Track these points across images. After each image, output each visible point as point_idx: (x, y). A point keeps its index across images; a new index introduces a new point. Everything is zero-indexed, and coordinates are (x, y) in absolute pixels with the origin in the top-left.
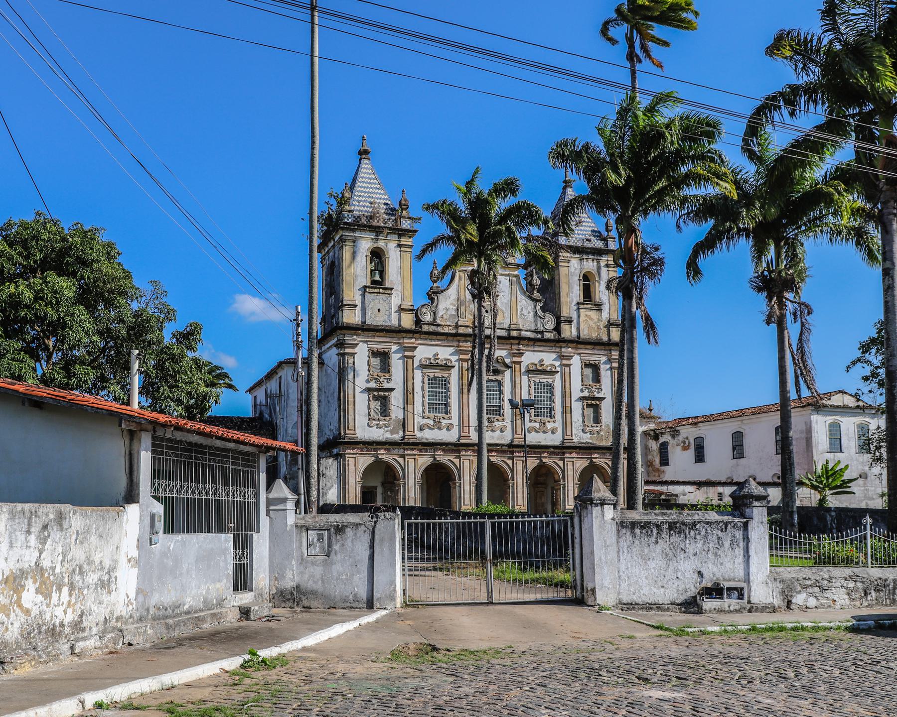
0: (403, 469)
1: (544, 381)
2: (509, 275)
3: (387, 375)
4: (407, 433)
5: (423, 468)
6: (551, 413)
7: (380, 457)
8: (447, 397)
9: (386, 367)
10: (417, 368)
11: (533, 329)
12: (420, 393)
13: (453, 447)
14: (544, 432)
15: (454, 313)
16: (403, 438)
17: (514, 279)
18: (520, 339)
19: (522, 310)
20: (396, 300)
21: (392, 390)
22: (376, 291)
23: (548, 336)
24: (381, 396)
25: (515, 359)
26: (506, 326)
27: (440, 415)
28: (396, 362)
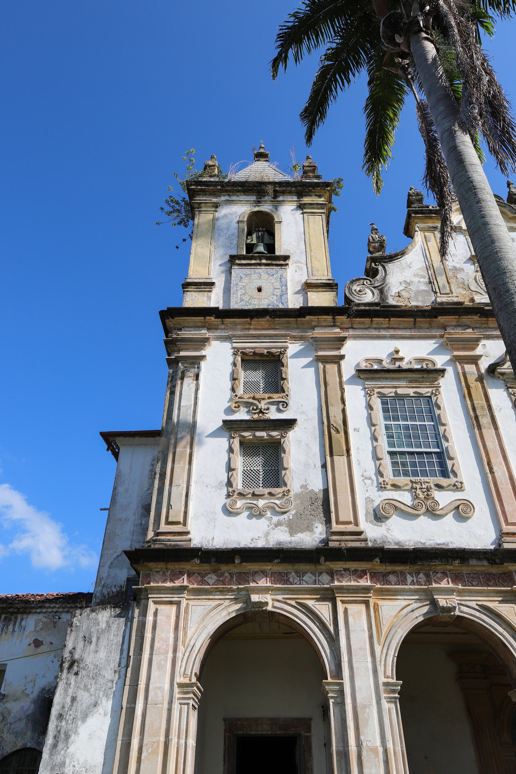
0: (333, 640)
3: (276, 397)
4: (335, 527)
5: (401, 634)
7: (255, 598)
9: (276, 383)
10: (351, 381)
12: (366, 431)
13: (483, 566)
15: (423, 287)
16: (326, 541)
20: (295, 275)
21: (290, 424)
22: (253, 262)
24: (261, 441)
28: (300, 374)
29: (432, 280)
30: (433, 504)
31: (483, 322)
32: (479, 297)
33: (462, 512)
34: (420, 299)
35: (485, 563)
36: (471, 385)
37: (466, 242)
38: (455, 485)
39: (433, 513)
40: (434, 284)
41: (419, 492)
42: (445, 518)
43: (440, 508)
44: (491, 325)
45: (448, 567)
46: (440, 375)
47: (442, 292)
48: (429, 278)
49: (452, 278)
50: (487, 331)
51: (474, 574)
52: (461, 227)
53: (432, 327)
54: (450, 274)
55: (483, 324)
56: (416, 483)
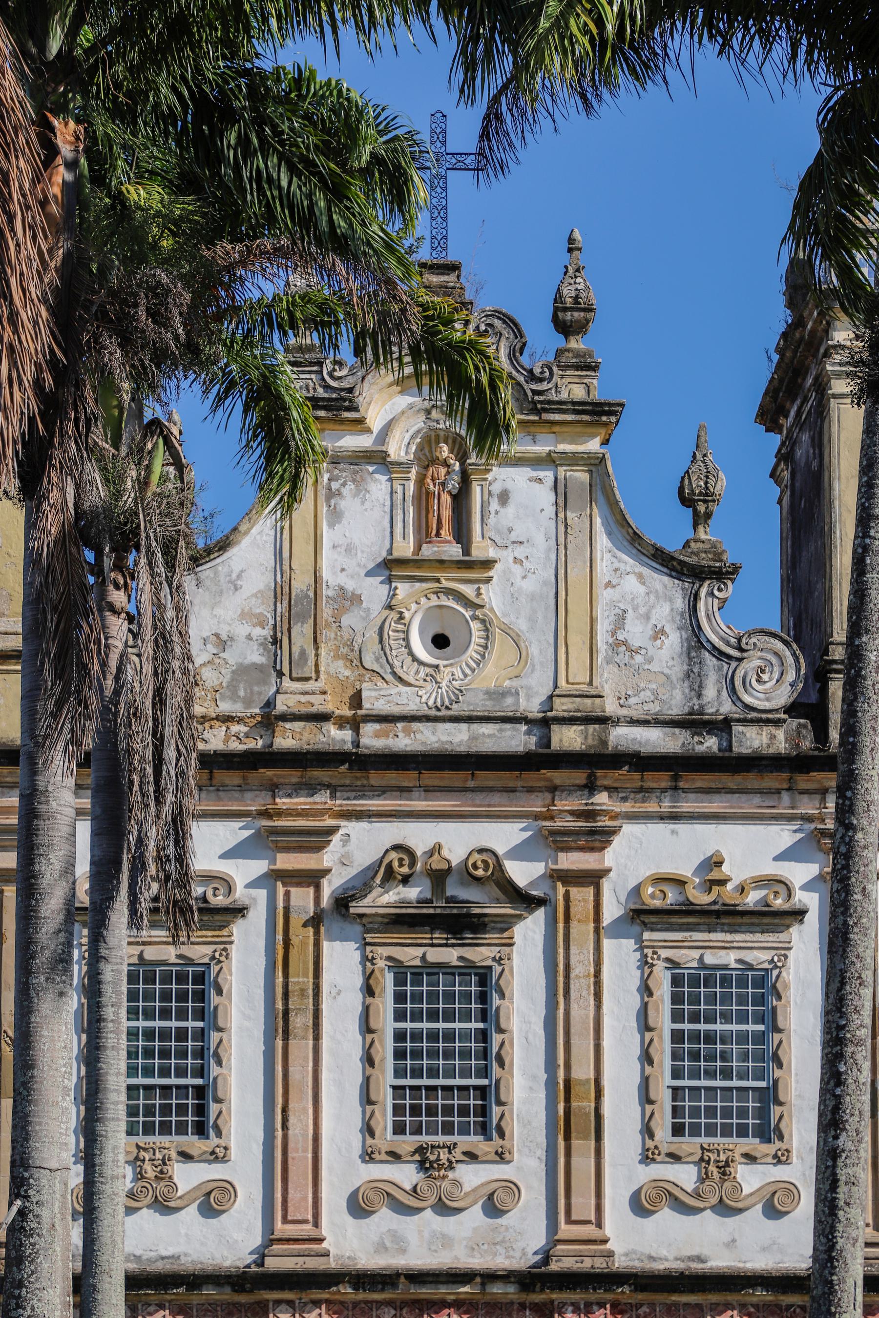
1: (730, 958)
2: (550, 461)
6: (763, 1113)
8: (204, 1054)
11: (677, 703)
14: (724, 1209)
15: (256, 656)
17: (581, 476)
18: (598, 764)
19: (620, 621)
23: (752, 740)
25: (570, 861)
26: (532, 706)
27: (171, 1142)
29: (279, 635)
30: (166, 1190)
31: (358, 775)
32: (374, 694)
33: (213, 1202)
34: (242, 693)
35: (228, 1289)
36: (295, 940)
37: (388, 503)
38: (213, 1153)
39: (164, 1206)
40: (281, 648)
41: (147, 1166)
42: (183, 1212)
43: (179, 1194)
44: (373, 782)
45: (168, 1297)
46: (236, 917)
47: (294, 675)
48: (275, 626)
49: (328, 625)
50: (362, 797)
51: (210, 1304)
52: (386, 454)
53: (247, 784)
54: (326, 612)
55: (357, 778)
56: (145, 1149)
